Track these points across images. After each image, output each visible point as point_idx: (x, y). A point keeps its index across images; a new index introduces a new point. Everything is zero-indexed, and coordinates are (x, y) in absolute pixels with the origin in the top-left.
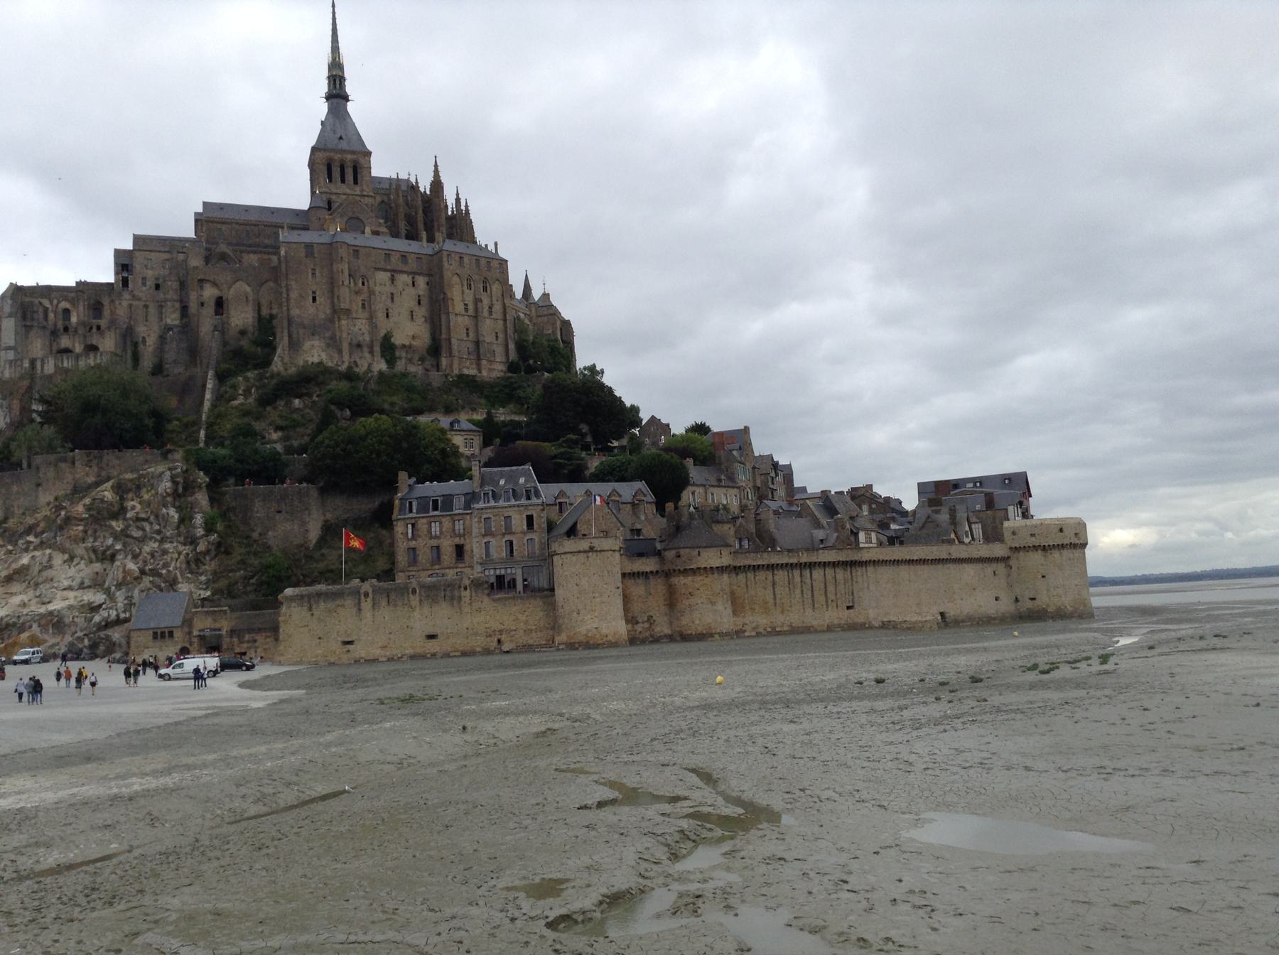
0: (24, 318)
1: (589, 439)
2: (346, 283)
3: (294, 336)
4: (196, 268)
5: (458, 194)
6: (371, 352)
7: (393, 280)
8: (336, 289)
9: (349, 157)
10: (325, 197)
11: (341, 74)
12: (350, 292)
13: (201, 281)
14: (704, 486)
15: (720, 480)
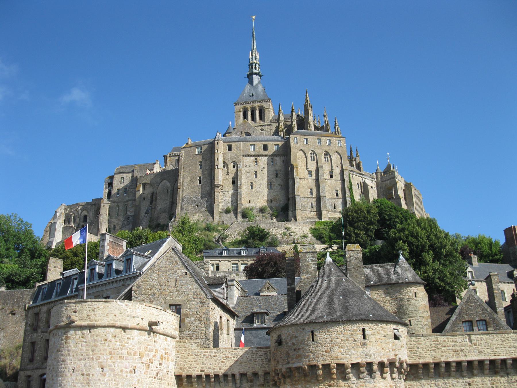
7: (256, 162)
8: (213, 171)
9: (256, 105)
11: (256, 62)
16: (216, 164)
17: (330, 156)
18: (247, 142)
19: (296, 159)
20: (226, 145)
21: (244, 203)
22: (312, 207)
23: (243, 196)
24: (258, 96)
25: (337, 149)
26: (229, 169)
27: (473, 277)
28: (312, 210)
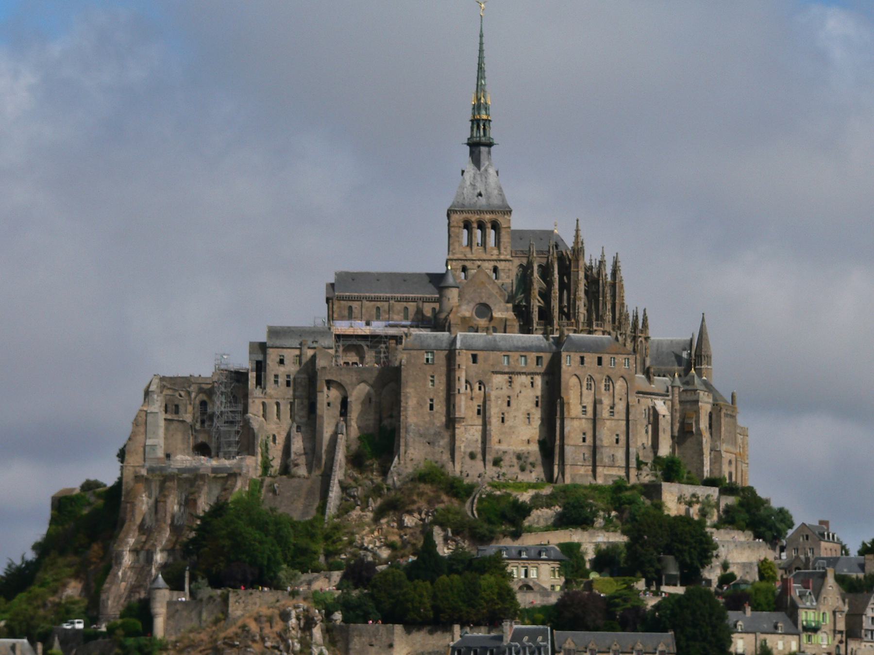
0: (166, 412)
1: (674, 571)
2: (461, 392)
3: (410, 444)
4: (324, 368)
5: (603, 256)
6: (484, 460)
8: (452, 398)
10: (459, 265)
11: (484, 117)
12: (466, 398)
13: (329, 383)
14: (755, 633)
15: (776, 627)
16: (457, 387)
17: (613, 383)
18: (499, 351)
19: (567, 389)
20: (470, 353)
21: (495, 447)
22: (584, 460)
23: (492, 433)
24: (489, 198)
25: (623, 372)
26: (473, 392)
27: (741, 629)
28: (584, 464)
